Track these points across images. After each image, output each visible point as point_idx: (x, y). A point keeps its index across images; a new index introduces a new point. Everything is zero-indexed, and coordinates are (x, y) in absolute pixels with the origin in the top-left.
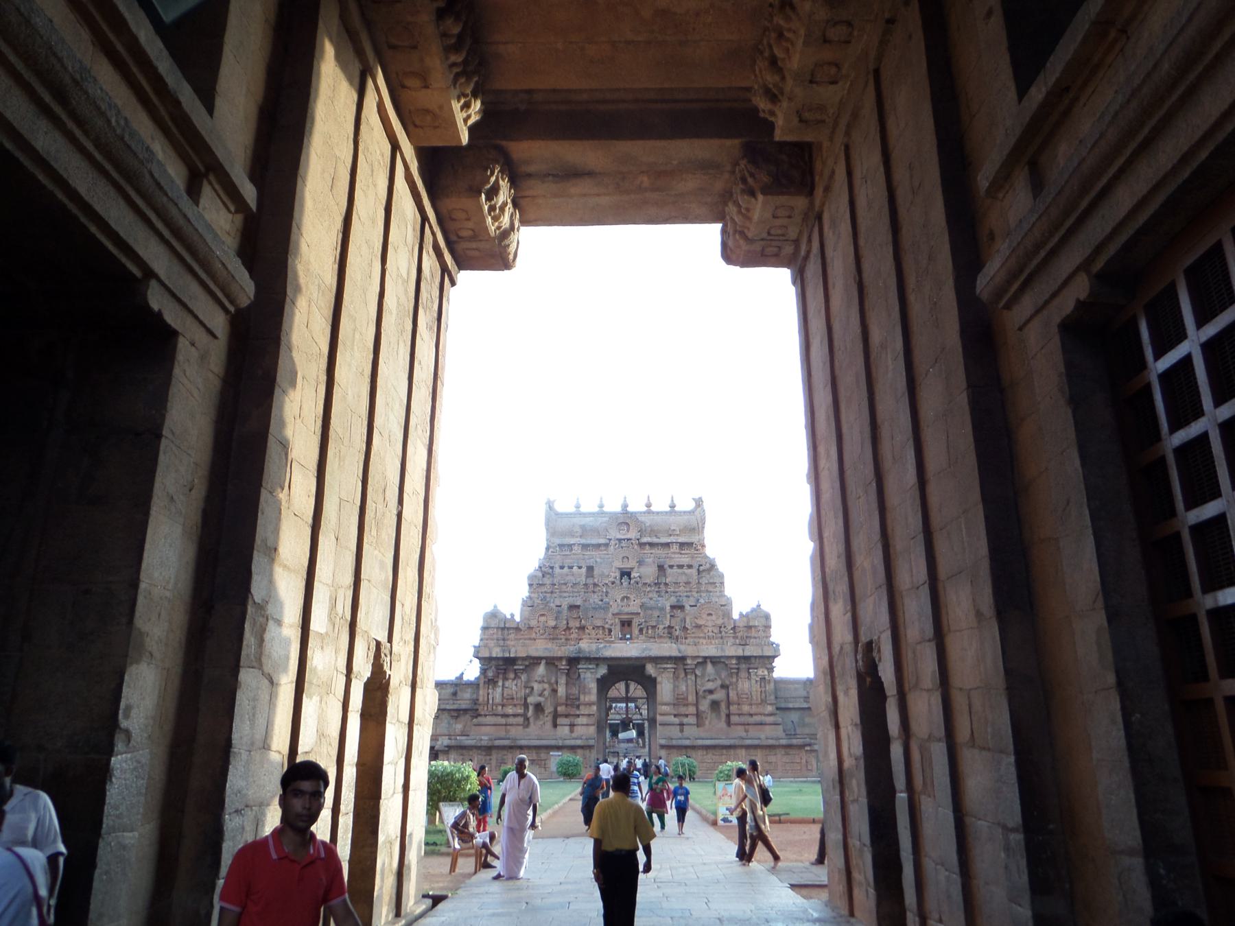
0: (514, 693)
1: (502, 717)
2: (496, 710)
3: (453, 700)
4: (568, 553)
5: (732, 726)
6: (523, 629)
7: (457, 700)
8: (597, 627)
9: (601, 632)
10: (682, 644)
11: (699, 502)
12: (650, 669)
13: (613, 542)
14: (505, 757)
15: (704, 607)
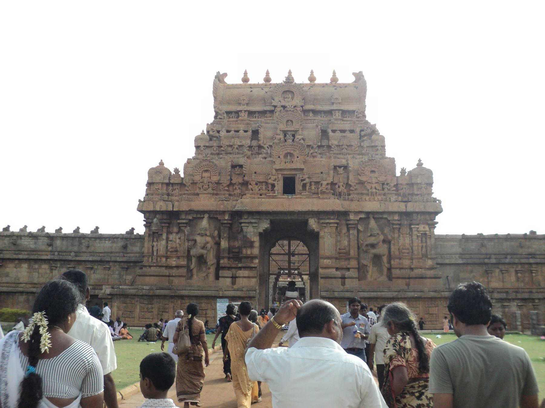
0: (178, 245)
1: (166, 269)
2: (160, 261)
3: (123, 252)
4: (235, 119)
5: (394, 280)
6: (188, 185)
7: (128, 253)
8: (260, 182)
9: (264, 187)
10: (345, 200)
11: (359, 77)
12: (313, 223)
13: (278, 109)
14: (167, 306)
15: (367, 164)
